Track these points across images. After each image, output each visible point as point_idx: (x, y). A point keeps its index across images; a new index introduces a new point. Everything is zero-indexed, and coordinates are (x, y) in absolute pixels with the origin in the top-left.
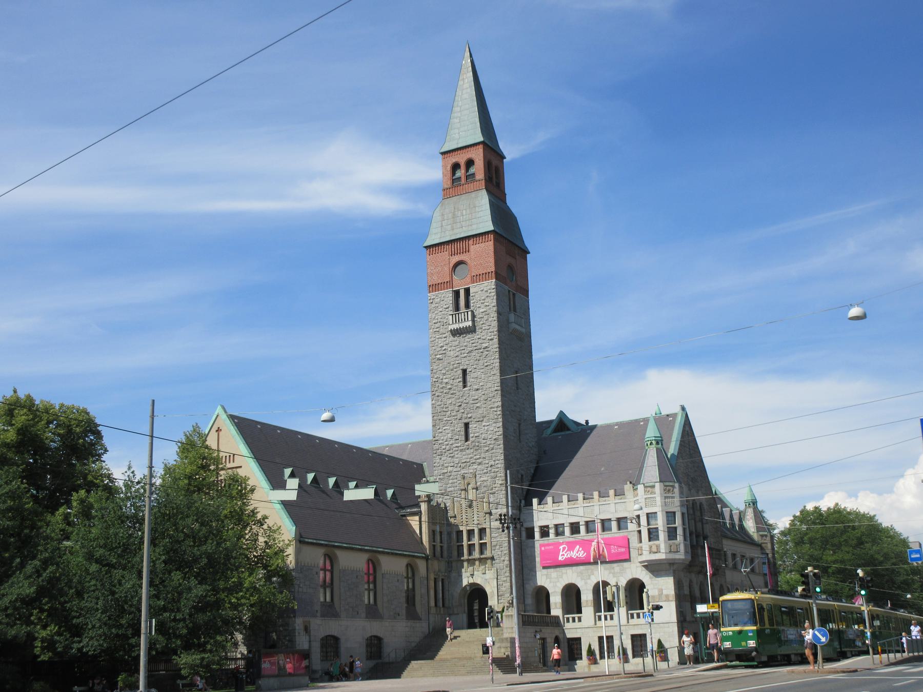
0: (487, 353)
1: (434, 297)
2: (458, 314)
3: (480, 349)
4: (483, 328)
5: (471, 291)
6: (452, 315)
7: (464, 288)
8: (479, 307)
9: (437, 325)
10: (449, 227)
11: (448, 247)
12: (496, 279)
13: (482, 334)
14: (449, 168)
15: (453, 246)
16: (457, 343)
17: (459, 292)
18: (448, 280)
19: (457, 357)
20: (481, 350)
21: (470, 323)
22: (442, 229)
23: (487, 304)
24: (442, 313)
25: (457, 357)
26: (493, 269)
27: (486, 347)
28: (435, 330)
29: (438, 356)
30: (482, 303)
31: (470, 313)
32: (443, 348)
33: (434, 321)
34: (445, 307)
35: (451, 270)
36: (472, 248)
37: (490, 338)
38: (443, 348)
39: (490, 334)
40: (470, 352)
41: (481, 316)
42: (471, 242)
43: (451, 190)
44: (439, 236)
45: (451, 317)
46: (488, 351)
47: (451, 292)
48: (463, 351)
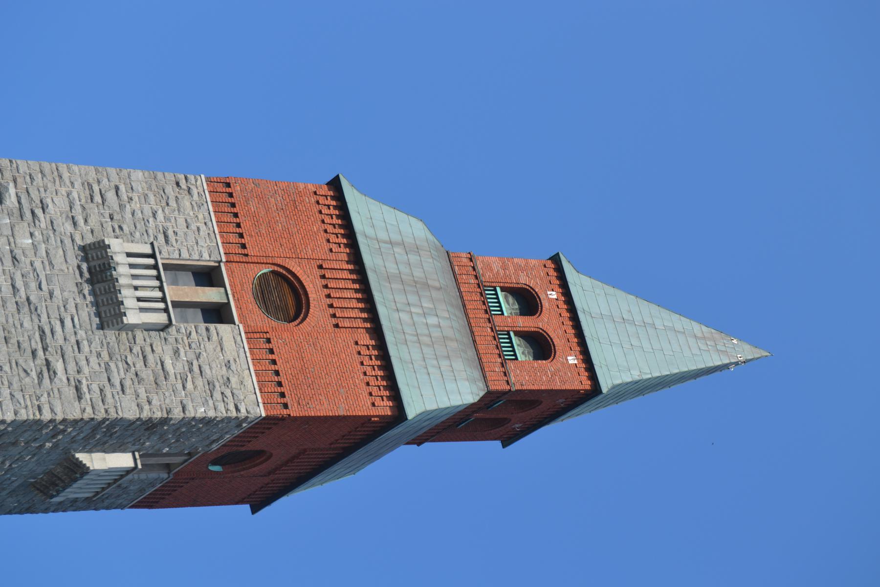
0: (34, 374)
1: (196, 197)
2: (158, 278)
3: (45, 349)
4: (112, 365)
5: (224, 328)
6: (153, 256)
7: (228, 303)
8: (176, 352)
9: (111, 196)
10: (392, 268)
11: (343, 253)
12: (267, 418)
13: (93, 360)
14: (523, 280)
15: (346, 275)
16: (58, 259)
17: (211, 285)
18: (250, 251)
19: (14, 258)
20: (40, 353)
21: (132, 317)
22: (385, 242)
23: (189, 385)
24: (151, 220)
25: (14, 258)
26: (294, 411)
27: (53, 374)
28: (96, 188)
29: (12, 190)
30: (191, 364)
31: (162, 318)
32: (39, 212)
33: (122, 188)
34: (170, 233)
35: (279, 261)
36: (345, 338)
37: (84, 389)
38: (39, 212)
39: (95, 387)
40: (34, 310)
41: (150, 357)
42: (366, 339)
43: (473, 281)
44: (370, 232)
45: (148, 250)
46: (40, 375)
47: (215, 257)
48: (33, 285)
